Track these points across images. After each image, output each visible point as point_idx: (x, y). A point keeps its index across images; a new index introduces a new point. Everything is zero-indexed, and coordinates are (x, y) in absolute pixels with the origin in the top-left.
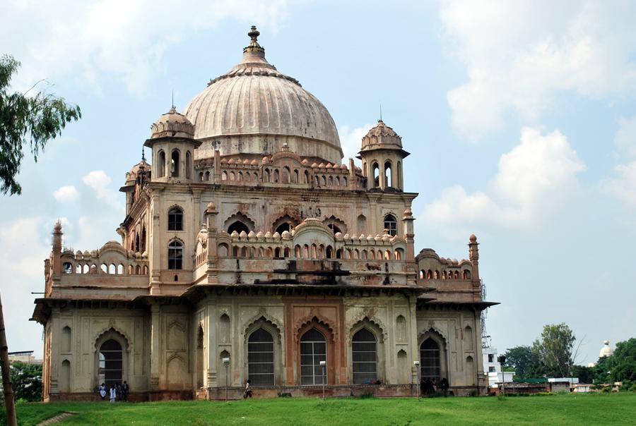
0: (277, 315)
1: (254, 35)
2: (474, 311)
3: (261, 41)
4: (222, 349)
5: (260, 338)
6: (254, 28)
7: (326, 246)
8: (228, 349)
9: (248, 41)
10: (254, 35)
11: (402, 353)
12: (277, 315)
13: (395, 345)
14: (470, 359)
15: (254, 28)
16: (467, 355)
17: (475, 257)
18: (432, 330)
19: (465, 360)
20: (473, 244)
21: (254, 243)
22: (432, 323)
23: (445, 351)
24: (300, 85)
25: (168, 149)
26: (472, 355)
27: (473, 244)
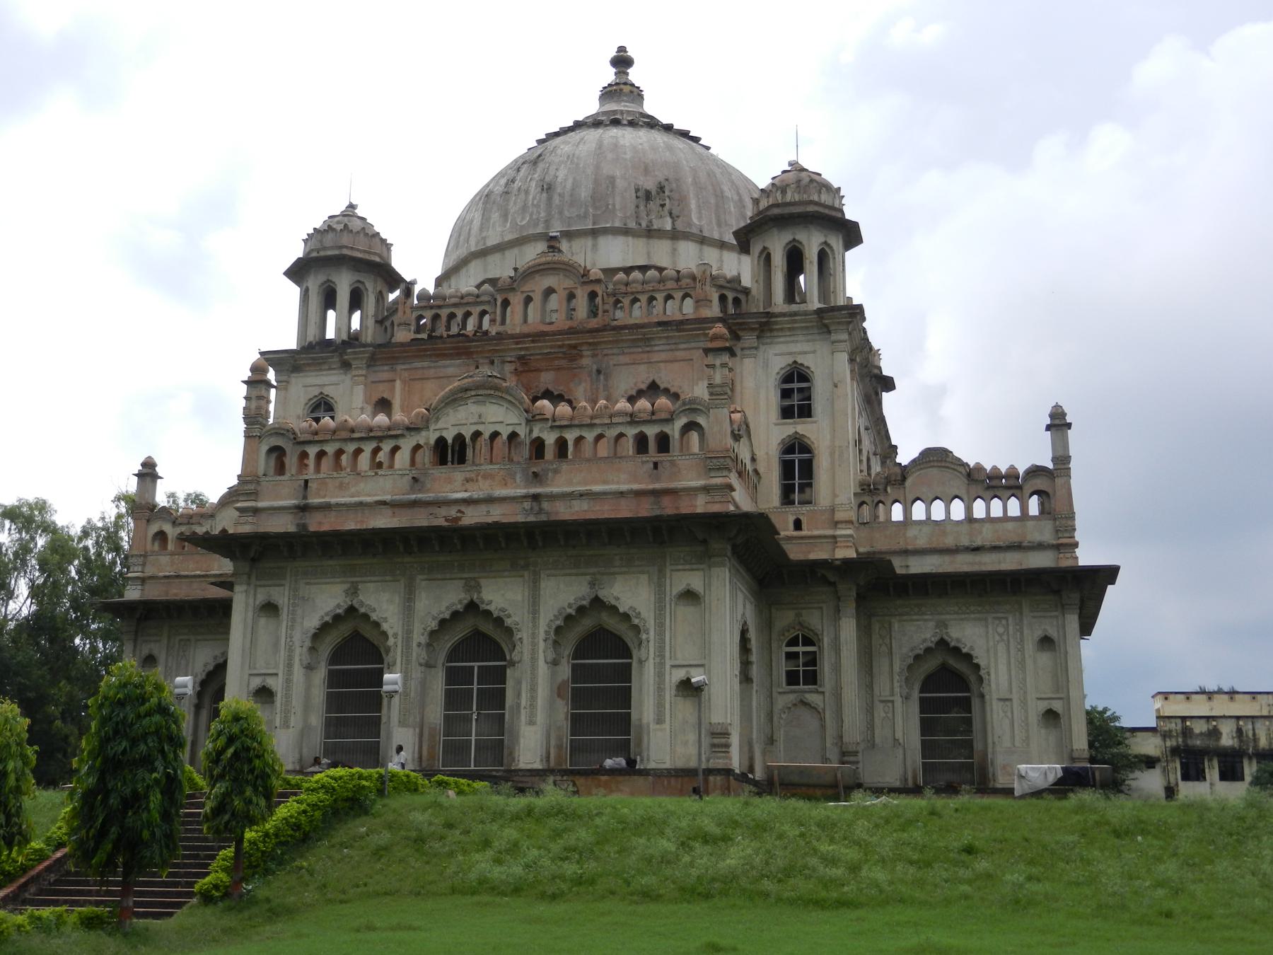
0: (382, 603)
1: (622, 61)
2: (1057, 592)
3: (634, 75)
4: (256, 682)
5: (353, 656)
6: (622, 49)
7: (505, 432)
8: (271, 682)
9: (609, 75)
10: (622, 61)
11: (688, 688)
12: (382, 603)
13: (668, 667)
14: (1051, 716)
15: (622, 49)
16: (1043, 706)
17: (1062, 460)
18: (942, 643)
19: (1034, 718)
20: (1058, 423)
21: (345, 440)
22: (943, 625)
23: (982, 696)
24: (696, 140)
25: (314, 282)
26: (1057, 706)
27: (1058, 423)
